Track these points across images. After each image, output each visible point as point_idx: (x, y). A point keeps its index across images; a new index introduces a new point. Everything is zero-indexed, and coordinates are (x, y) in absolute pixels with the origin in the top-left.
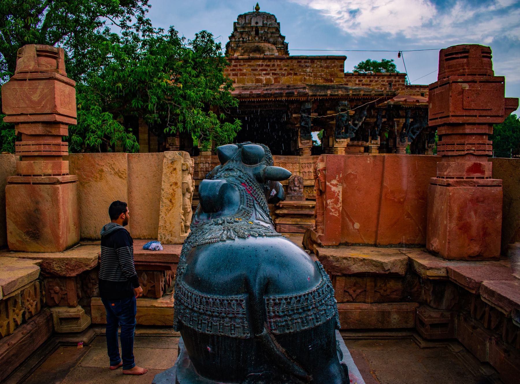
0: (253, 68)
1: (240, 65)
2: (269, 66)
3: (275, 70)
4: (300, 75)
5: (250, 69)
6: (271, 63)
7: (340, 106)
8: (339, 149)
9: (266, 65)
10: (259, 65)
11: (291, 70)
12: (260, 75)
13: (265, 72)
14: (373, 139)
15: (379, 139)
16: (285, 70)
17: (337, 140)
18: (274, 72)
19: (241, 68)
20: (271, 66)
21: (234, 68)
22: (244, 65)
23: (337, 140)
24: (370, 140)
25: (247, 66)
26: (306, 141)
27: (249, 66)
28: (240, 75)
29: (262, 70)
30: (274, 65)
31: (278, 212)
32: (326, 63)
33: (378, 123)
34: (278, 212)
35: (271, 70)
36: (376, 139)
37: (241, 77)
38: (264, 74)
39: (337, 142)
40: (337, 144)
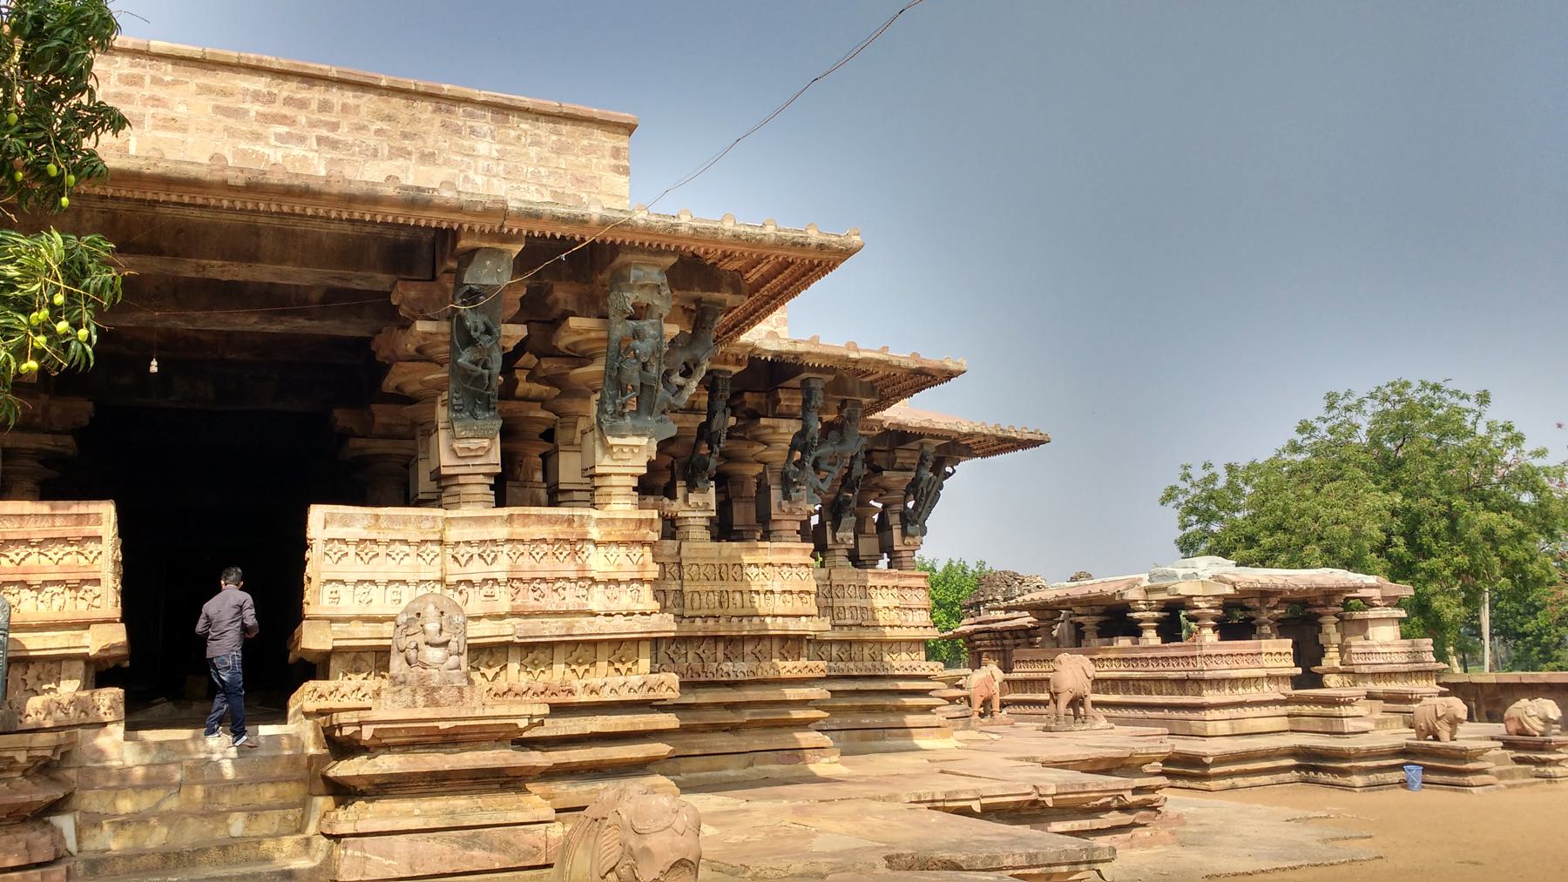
0: (225, 102)
1: (156, 81)
2: (302, 104)
3: (334, 127)
4: (447, 162)
5: (206, 103)
6: (316, 94)
7: (631, 288)
8: (614, 480)
9: (288, 101)
10: (256, 96)
11: (405, 136)
12: (257, 137)
13: (283, 129)
14: (691, 487)
15: (712, 491)
16: (379, 132)
17: (611, 440)
18: (324, 132)
19: (158, 91)
20: (314, 106)
21: (126, 89)
22: (175, 82)
23: (611, 440)
24: (680, 492)
25: (192, 87)
26: (474, 444)
27: (208, 90)
28: (156, 127)
29: (266, 118)
30: (325, 107)
31: (345, 769)
32: (559, 134)
33: (714, 428)
34: (345, 769)
35: (313, 124)
36: (705, 491)
37: (161, 134)
38: (279, 137)
39: (608, 449)
40: (607, 461)
